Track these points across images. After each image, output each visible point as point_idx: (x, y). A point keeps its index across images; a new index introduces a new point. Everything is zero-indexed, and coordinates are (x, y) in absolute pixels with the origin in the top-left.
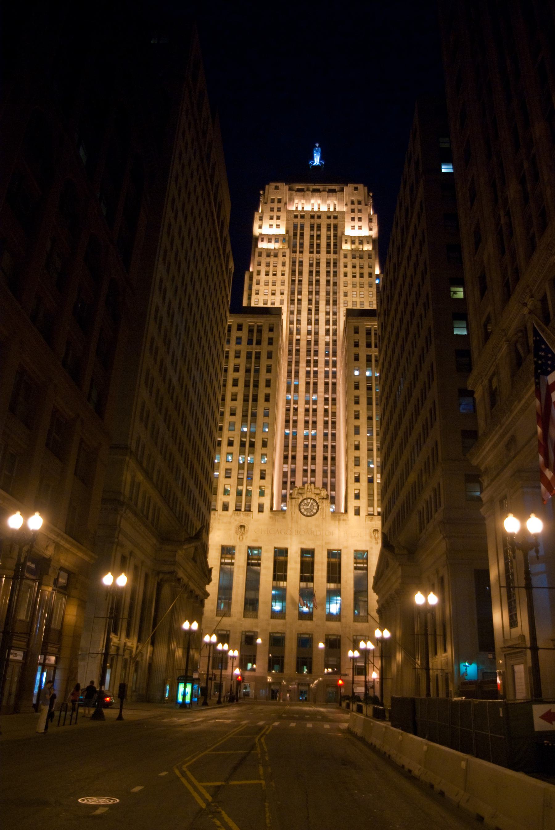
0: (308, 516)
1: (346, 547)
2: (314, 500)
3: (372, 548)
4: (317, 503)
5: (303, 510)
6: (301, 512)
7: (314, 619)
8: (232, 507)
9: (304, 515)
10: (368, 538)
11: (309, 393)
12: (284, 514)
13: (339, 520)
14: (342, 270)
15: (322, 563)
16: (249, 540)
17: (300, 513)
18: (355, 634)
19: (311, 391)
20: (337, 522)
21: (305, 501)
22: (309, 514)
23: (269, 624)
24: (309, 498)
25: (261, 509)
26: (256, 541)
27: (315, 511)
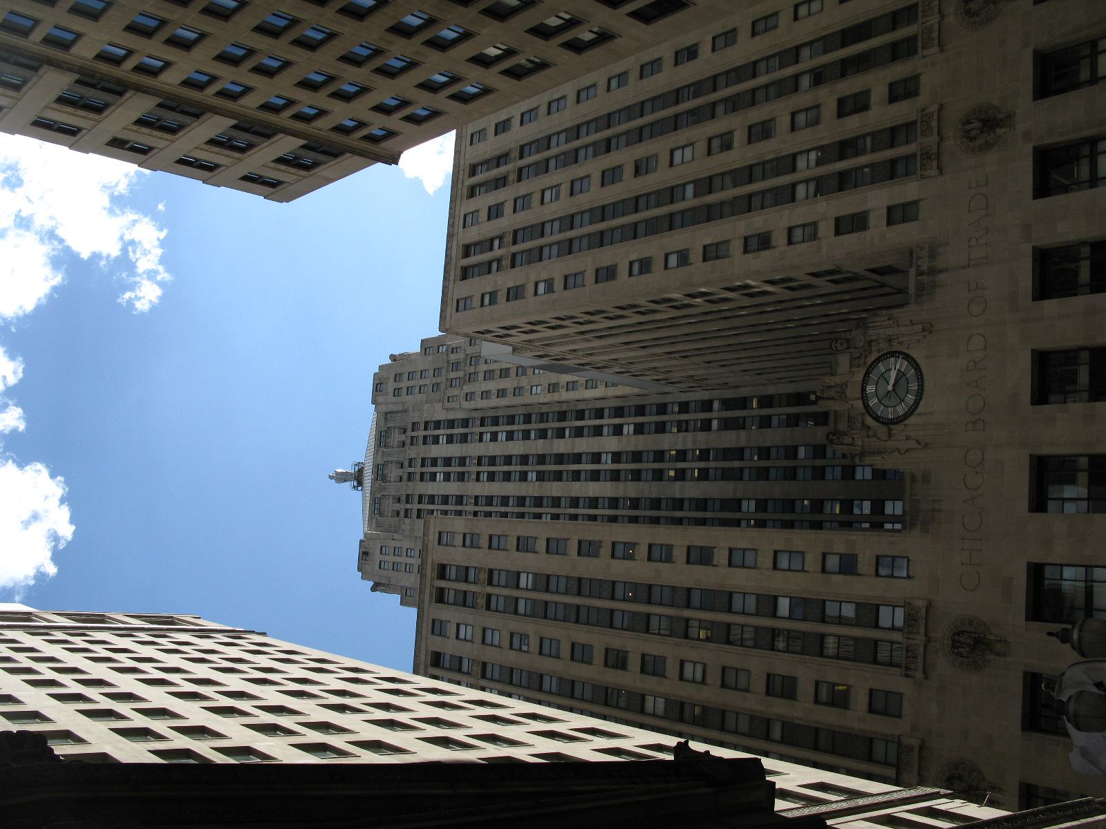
2: (867, 374)
4: (878, 360)
5: (901, 410)
6: (906, 416)
11: (741, 469)
12: (913, 478)
13: (933, 271)
14: (494, 402)
16: (1007, 612)
17: (912, 420)
19: (737, 464)
20: (941, 277)
21: (873, 402)
22: (914, 387)
24: (863, 390)
27: (901, 364)
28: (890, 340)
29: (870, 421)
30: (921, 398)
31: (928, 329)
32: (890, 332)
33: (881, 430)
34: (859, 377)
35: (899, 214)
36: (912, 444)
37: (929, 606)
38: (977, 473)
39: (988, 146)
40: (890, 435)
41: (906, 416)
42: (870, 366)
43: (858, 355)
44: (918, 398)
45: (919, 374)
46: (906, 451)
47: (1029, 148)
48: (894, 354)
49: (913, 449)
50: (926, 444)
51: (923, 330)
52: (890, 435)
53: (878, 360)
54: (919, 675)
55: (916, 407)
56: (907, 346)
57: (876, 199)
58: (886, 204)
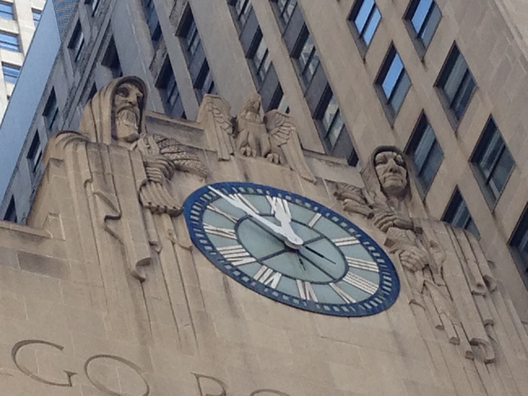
28: (427, 267)
30: (275, 300)
36: (138, 251)
38: (70, 375)
40: (157, 211)
42: (342, 219)
43: (371, 202)
44: (275, 294)
45: (345, 309)
46: (112, 234)
49: (123, 253)
50: (142, 280)
51: (474, 343)
52: (157, 211)
55: (246, 285)
56: (419, 300)
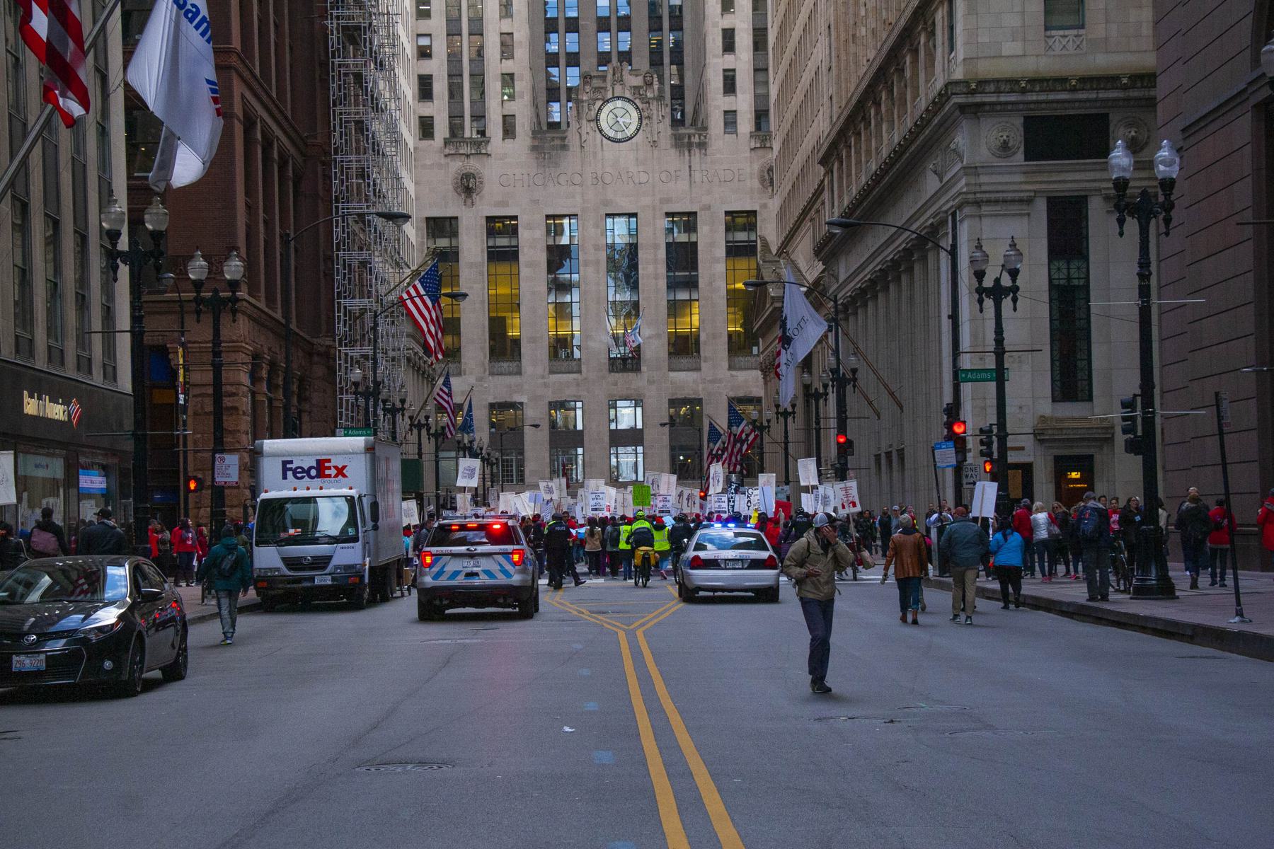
0: (619, 141)
1: (708, 208)
3: (764, 206)
7: (644, 368)
8: (441, 129)
9: (609, 138)
10: (756, 184)
13: (690, 145)
15: (656, 246)
16: (487, 206)
17: (599, 135)
18: (732, 394)
21: (610, 106)
22: (619, 136)
23: (546, 385)
24: (618, 98)
25: (509, 130)
26: (503, 204)
27: (633, 128)
28: (649, 117)
29: (599, 103)
31: (654, 144)
32: (655, 117)
33: (593, 113)
34: (628, 95)
35: (730, 118)
37: (489, 155)
39: (762, 181)
41: (601, 131)
47: (756, 208)
48: (640, 119)
53: (637, 108)
54: (447, 151)
57: (744, 103)
58: (739, 109)
